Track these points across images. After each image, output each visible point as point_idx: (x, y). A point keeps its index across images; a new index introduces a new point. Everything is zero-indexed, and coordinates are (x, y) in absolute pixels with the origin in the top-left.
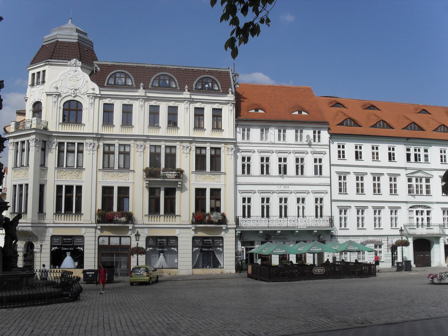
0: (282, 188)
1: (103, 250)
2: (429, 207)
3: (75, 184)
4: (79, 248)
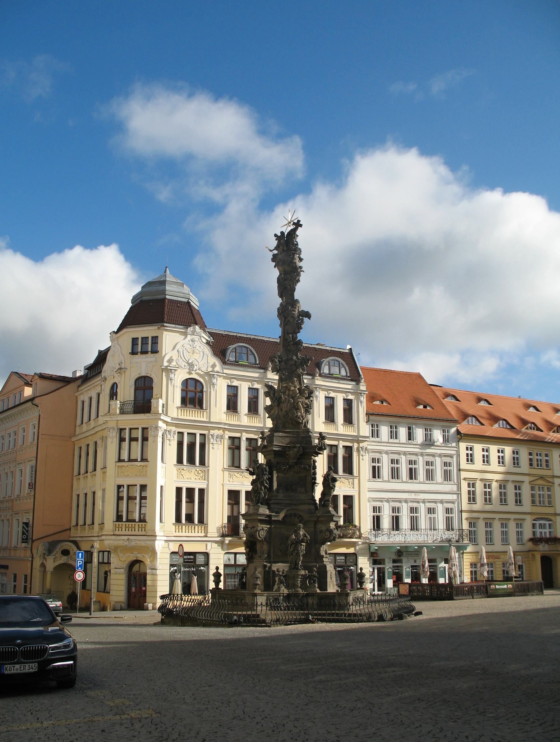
0: (413, 496)
2: (550, 520)
3: (197, 485)
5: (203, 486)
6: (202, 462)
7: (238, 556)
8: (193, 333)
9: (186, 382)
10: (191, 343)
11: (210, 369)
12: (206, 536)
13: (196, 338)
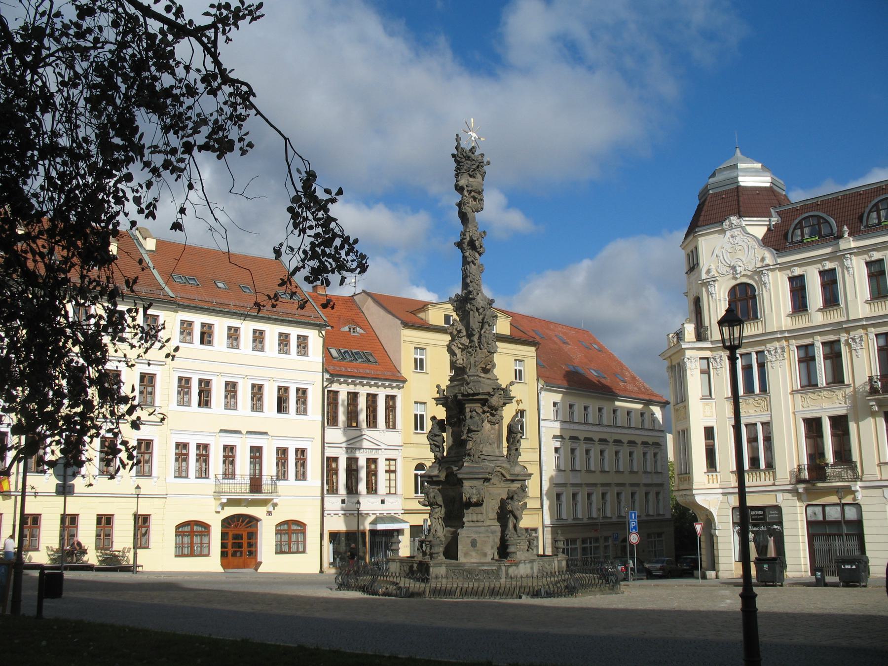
1: (818, 530)
4: (775, 527)
5: (766, 419)
6: (764, 388)
7: (827, 509)
8: (731, 227)
9: (733, 291)
10: (731, 240)
11: (759, 265)
12: (774, 485)
13: (736, 232)
